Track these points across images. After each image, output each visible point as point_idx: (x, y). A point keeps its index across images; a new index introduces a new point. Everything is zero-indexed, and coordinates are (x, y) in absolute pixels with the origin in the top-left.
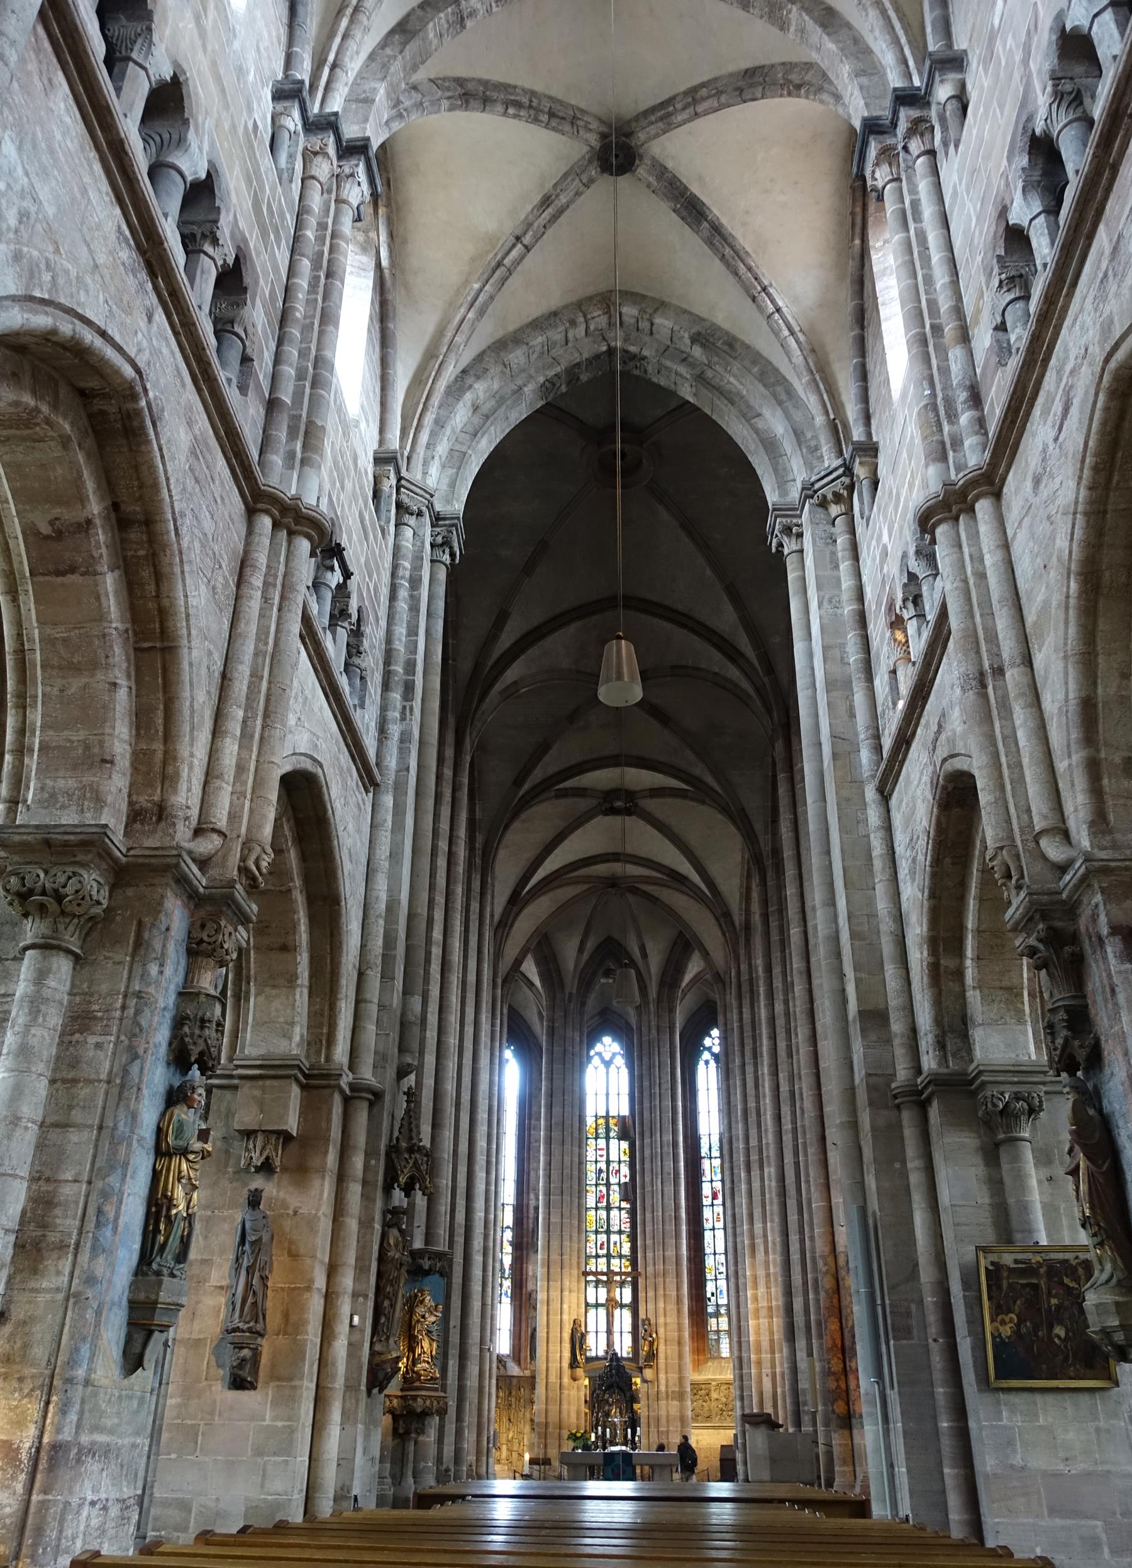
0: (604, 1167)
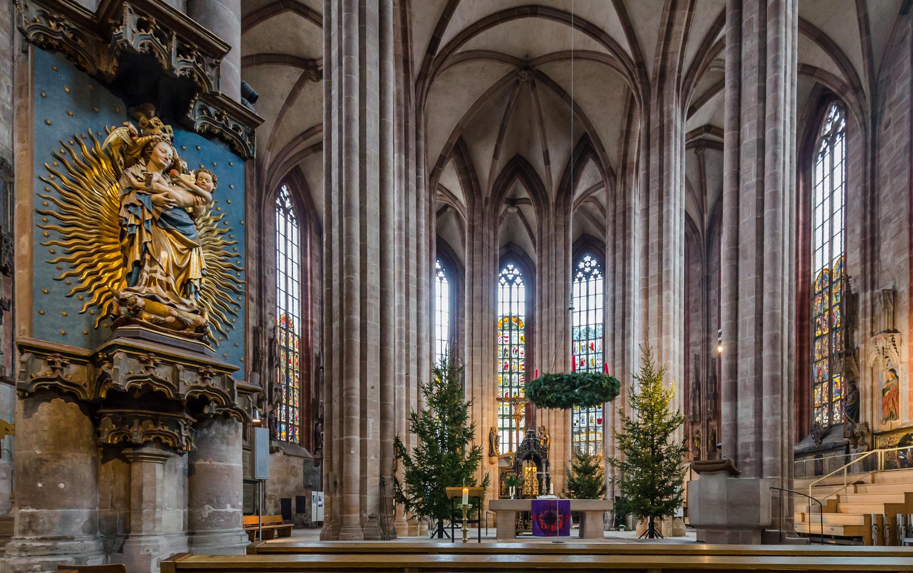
0: (508, 347)
